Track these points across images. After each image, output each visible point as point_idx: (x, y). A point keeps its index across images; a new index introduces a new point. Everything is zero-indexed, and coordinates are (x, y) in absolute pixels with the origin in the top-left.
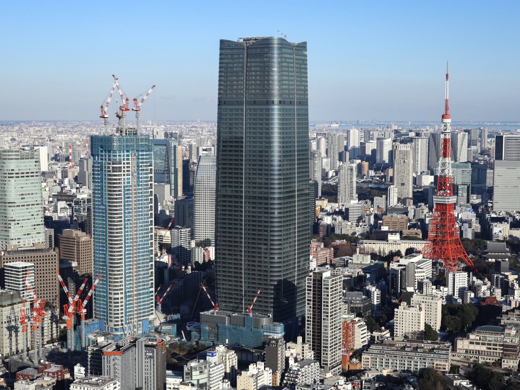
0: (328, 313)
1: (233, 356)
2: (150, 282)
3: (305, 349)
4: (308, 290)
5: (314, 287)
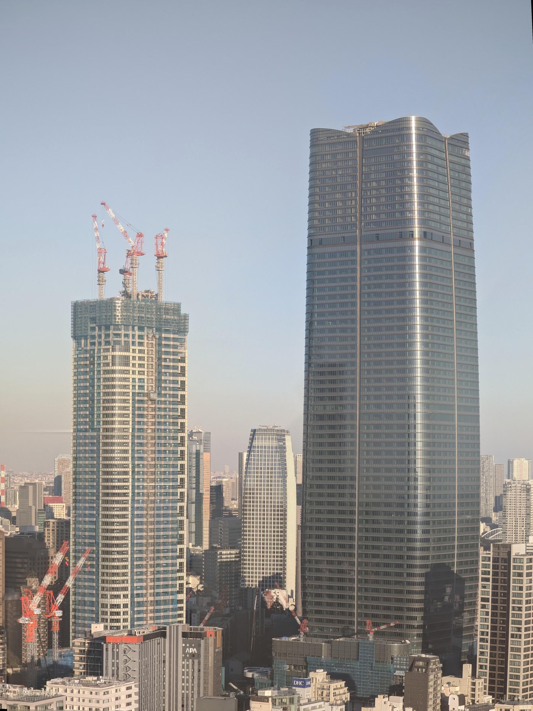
0: (520, 623)
1: (342, 691)
3: (477, 687)
4: (484, 580)
5: (495, 574)
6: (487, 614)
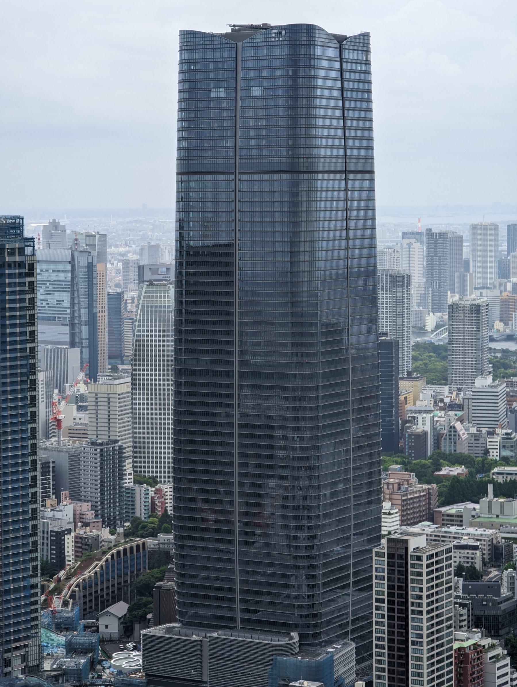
2: (31, 564)
6: (383, 616)
